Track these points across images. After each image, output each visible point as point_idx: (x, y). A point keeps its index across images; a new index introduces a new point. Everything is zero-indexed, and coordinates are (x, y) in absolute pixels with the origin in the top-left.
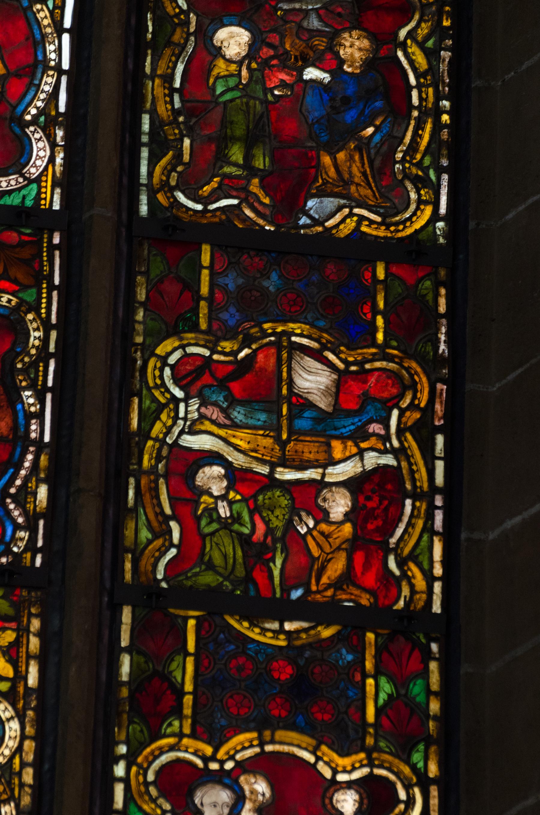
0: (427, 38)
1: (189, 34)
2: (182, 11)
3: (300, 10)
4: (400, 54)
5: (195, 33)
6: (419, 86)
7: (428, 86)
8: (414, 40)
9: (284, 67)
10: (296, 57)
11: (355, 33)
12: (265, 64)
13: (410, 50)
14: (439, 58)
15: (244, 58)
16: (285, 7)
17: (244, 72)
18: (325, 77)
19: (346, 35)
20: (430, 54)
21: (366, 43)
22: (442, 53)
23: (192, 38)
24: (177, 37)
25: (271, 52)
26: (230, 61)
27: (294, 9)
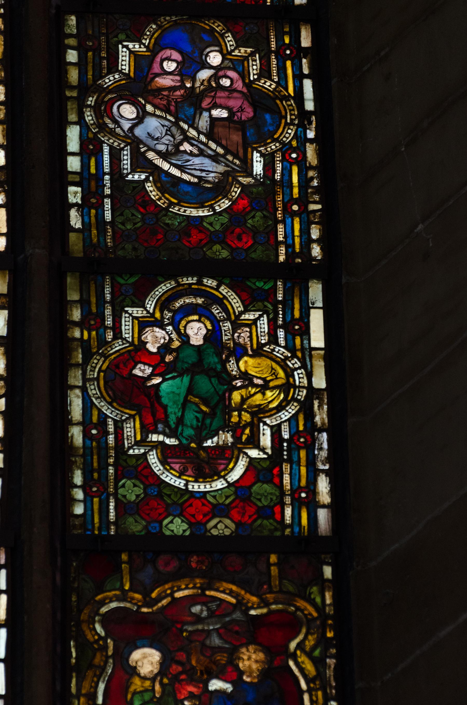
0: (314, 648)
1: (107, 657)
2: (100, 637)
3: (203, 630)
4: (291, 663)
5: (113, 656)
6: (310, 691)
7: (317, 690)
8: (303, 651)
9: (192, 681)
10: (201, 672)
11: (251, 648)
12: (175, 679)
13: (300, 660)
14: (325, 665)
15: (156, 675)
16: (190, 628)
17: (157, 687)
18: (228, 687)
19: (244, 650)
20: (317, 662)
21: (261, 656)
22: (328, 660)
23: (111, 661)
24: (98, 660)
25: (180, 669)
26: (144, 678)
27: (197, 630)
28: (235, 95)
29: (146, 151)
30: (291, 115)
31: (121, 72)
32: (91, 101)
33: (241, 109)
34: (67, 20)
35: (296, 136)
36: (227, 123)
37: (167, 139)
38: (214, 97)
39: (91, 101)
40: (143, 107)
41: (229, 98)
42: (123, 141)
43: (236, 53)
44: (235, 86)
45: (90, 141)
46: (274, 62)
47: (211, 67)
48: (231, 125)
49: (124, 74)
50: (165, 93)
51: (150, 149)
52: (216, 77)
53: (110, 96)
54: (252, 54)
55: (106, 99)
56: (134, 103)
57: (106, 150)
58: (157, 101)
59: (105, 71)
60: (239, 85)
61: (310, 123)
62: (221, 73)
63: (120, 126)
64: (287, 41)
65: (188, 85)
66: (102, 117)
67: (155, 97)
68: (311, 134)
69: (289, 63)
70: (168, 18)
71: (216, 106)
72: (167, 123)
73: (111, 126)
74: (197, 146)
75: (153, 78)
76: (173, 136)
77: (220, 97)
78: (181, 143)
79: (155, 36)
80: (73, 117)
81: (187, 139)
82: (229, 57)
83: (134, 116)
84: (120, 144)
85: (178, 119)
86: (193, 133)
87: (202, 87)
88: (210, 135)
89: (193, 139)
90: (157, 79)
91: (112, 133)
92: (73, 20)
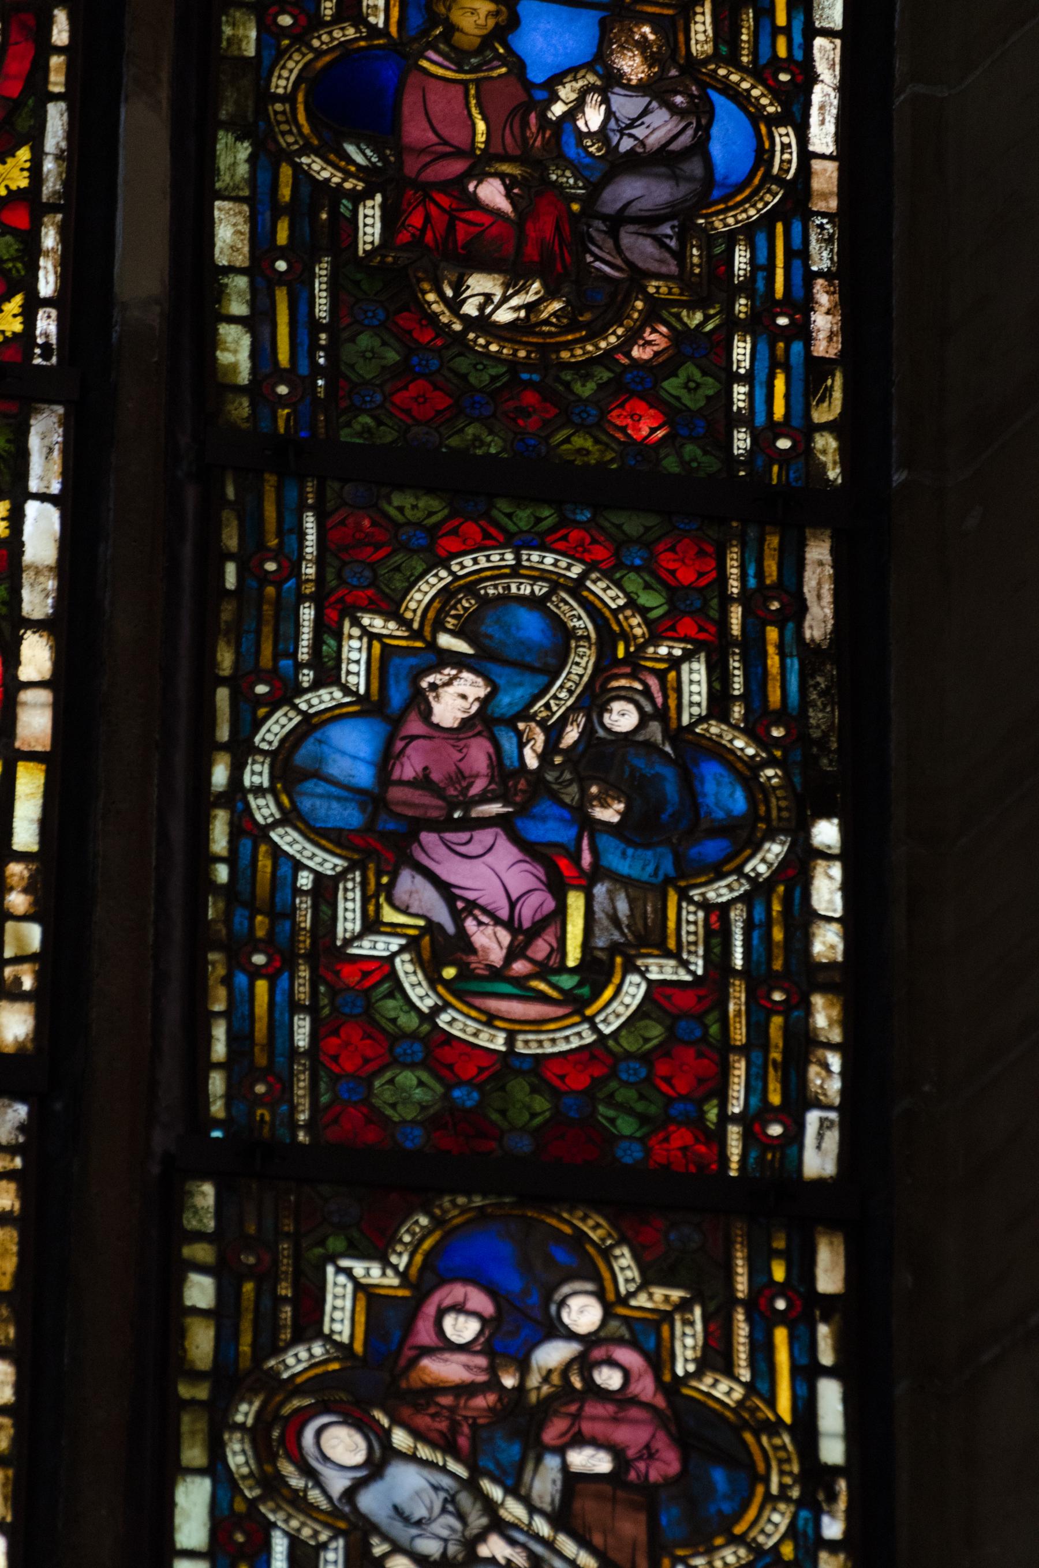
28: (634, 1413)
29: (386, 1556)
30: (782, 1473)
31: (328, 1339)
32: (245, 1413)
33: (649, 1453)
34: (191, 1194)
35: (792, 1532)
36: (607, 1489)
37: (445, 1525)
38: (576, 1417)
39: (245, 1413)
40: (385, 1436)
41: (615, 1420)
42: (327, 1525)
43: (641, 1300)
44: (635, 1388)
45: (237, 1521)
46: (742, 1330)
47: (571, 1336)
48: (620, 1494)
49: (338, 1345)
50: (446, 1400)
51: (397, 1549)
52: (584, 1363)
53: (296, 1403)
54: (684, 1306)
55: (286, 1410)
56: (362, 1424)
57: (280, 1545)
58: (423, 1421)
59: (286, 1335)
60: (645, 1387)
61: (832, 1497)
62: (598, 1353)
63: (319, 1484)
64: (779, 1273)
65: (509, 1381)
66: (273, 1458)
67: (418, 1409)
68: (833, 1529)
69: (781, 1335)
70: (461, 1200)
71: (579, 1440)
72: (446, 1482)
73: (296, 1482)
74: (524, 1546)
75: (414, 1361)
76: (461, 1517)
77: (594, 1418)
78: (482, 1537)
79: (427, 1245)
80: (194, 1454)
81: (499, 1526)
82: (622, 1311)
83: (359, 1458)
84: (316, 1534)
85: (476, 1472)
86: (514, 1510)
87: (546, 1389)
88: (560, 1520)
89: (515, 1526)
90: (426, 1362)
91: (299, 1502)
92: (206, 1194)
